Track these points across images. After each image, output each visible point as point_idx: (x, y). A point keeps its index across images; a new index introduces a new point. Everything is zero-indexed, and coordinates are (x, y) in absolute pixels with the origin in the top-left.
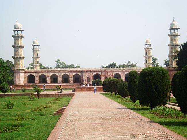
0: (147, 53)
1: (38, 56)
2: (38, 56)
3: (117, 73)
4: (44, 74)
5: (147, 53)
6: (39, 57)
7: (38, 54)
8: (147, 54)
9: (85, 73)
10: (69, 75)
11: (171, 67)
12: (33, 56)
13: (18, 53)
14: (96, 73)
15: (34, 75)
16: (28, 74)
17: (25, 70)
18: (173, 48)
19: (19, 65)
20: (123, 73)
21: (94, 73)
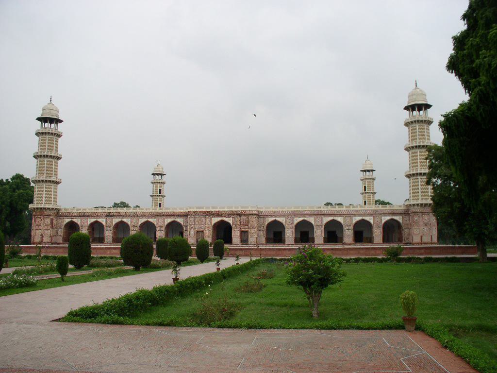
0: (365, 187)
1: (160, 193)
2: (160, 193)
3: (275, 221)
4: (100, 220)
5: (365, 187)
6: (162, 195)
7: (160, 190)
8: (365, 190)
9: (192, 219)
10: (155, 224)
11: (414, 205)
12: (152, 194)
13: (42, 170)
14: (220, 219)
15: (79, 223)
16: (67, 220)
17: (61, 211)
18: (418, 154)
19: (42, 197)
20: (289, 220)
21: (216, 220)
